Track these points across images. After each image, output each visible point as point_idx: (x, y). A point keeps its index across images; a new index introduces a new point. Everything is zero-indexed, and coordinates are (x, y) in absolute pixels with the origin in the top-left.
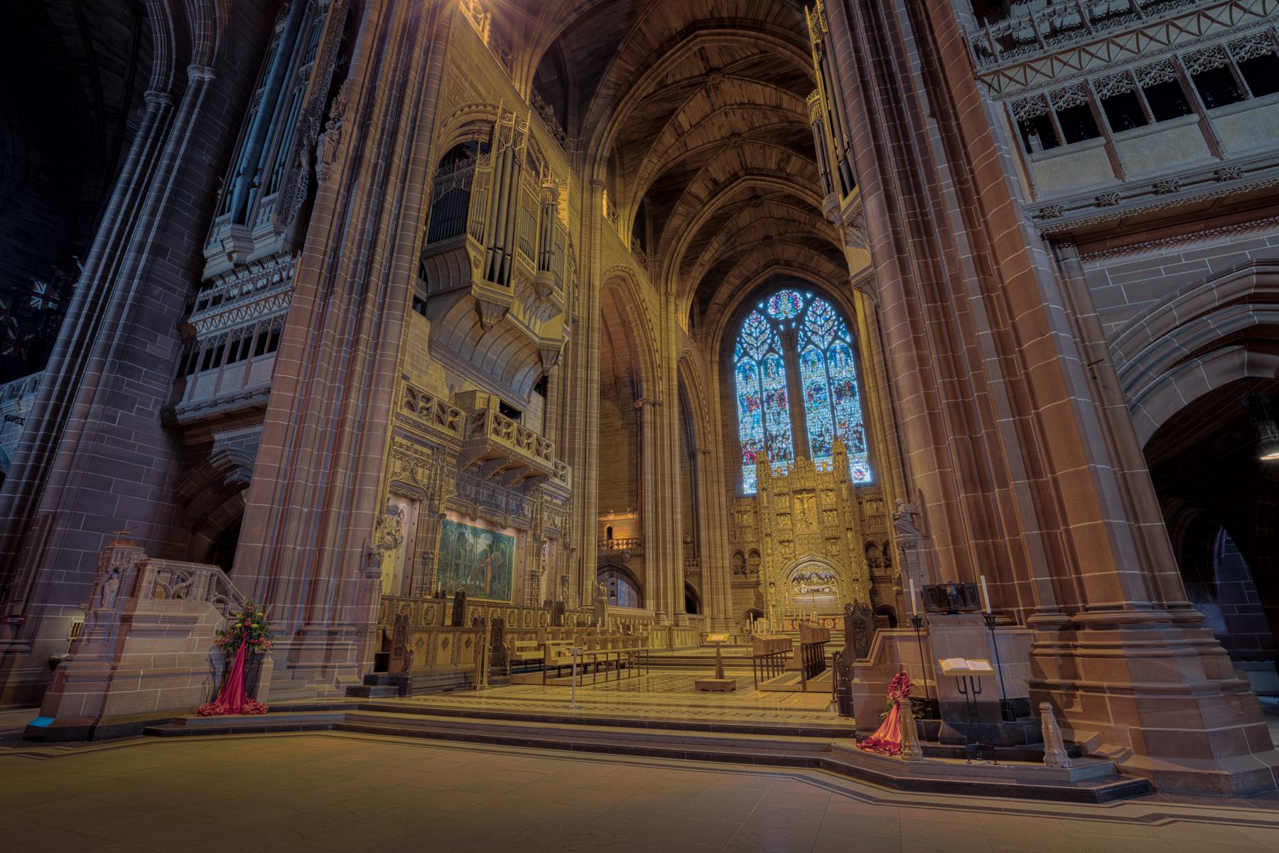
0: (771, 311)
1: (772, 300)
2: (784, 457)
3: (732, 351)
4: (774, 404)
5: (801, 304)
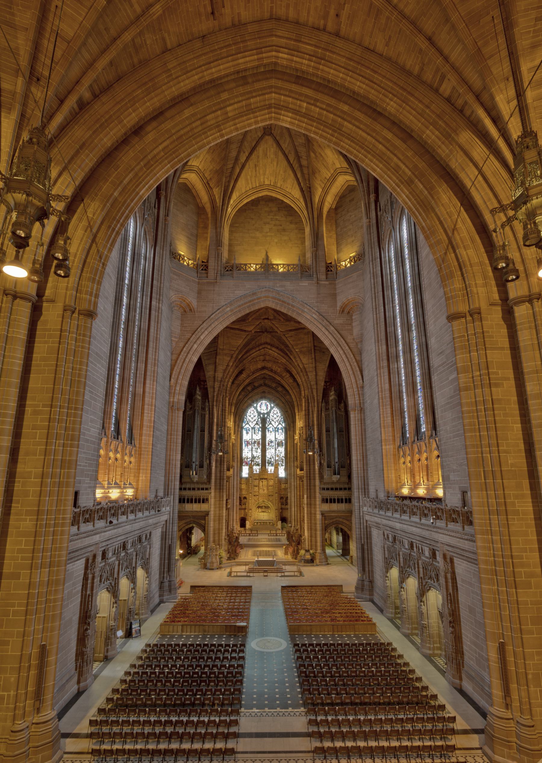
0: (259, 408)
1: (259, 404)
2: (258, 465)
3: (243, 422)
4: (256, 445)
5: (269, 408)
